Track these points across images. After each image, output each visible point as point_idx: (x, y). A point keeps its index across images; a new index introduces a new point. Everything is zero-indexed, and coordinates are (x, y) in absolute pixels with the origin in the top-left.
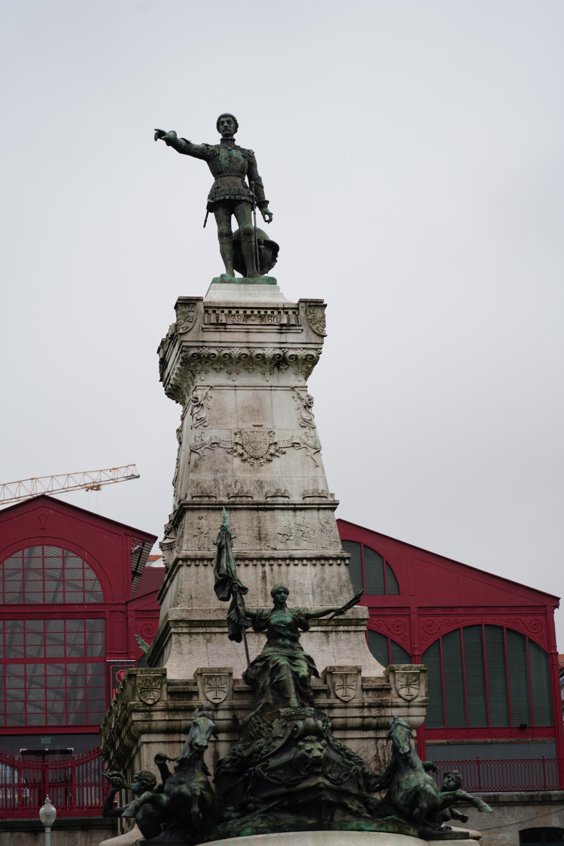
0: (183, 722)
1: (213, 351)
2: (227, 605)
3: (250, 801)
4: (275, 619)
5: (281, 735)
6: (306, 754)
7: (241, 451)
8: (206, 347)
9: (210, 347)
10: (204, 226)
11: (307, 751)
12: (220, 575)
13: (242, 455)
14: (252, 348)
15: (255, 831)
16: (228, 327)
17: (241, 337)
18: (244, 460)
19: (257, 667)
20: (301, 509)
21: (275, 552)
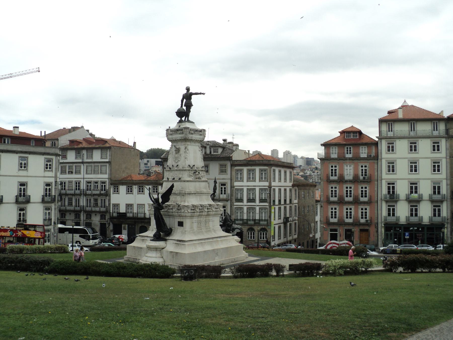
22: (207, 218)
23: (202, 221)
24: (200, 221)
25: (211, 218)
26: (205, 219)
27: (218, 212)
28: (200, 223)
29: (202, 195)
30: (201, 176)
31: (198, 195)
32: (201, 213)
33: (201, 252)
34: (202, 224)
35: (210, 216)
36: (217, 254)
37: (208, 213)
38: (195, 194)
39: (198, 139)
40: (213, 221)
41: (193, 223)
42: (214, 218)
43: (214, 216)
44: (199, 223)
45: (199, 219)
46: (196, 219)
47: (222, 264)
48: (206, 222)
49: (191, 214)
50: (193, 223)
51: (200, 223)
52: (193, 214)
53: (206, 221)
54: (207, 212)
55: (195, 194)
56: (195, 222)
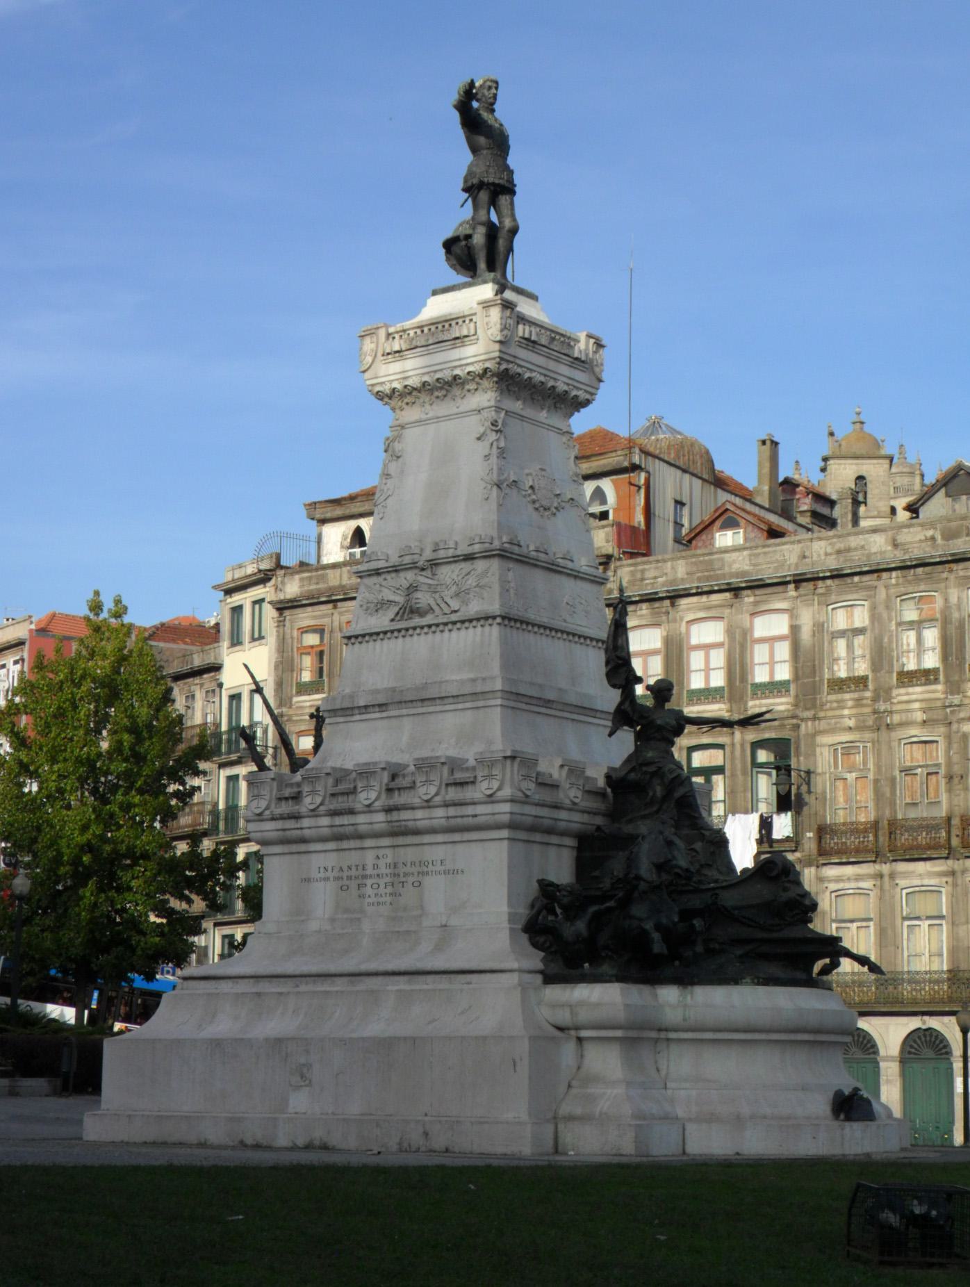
0: (545, 820)
1: (519, 370)
5: (711, 863)
6: (798, 898)
7: (534, 497)
8: (516, 364)
10: (462, 206)
11: (799, 895)
12: (619, 658)
13: (534, 502)
14: (548, 376)
15: (756, 981)
16: (537, 346)
17: (540, 360)
18: (537, 509)
19: (646, 773)
20: (582, 578)
21: (564, 624)
22: (409, 854)
23: (369, 871)
24: (353, 872)
25: (436, 852)
26: (389, 860)
27: (470, 810)
28: (353, 884)
29: (431, 709)
30: (457, 595)
31: (404, 712)
32: (345, 820)
34: (369, 891)
35: (427, 839)
36: (303, 1074)
37: (395, 816)
38: (382, 706)
40: (456, 872)
41: (307, 880)
42: (460, 848)
43: (457, 837)
45: (353, 858)
46: (331, 860)
47: (317, 1143)
48: (397, 878)
49: (279, 824)
50: (307, 880)
51: (353, 884)
52: (290, 824)
53: (402, 870)
54: (389, 810)
55: (382, 706)
56: (322, 875)
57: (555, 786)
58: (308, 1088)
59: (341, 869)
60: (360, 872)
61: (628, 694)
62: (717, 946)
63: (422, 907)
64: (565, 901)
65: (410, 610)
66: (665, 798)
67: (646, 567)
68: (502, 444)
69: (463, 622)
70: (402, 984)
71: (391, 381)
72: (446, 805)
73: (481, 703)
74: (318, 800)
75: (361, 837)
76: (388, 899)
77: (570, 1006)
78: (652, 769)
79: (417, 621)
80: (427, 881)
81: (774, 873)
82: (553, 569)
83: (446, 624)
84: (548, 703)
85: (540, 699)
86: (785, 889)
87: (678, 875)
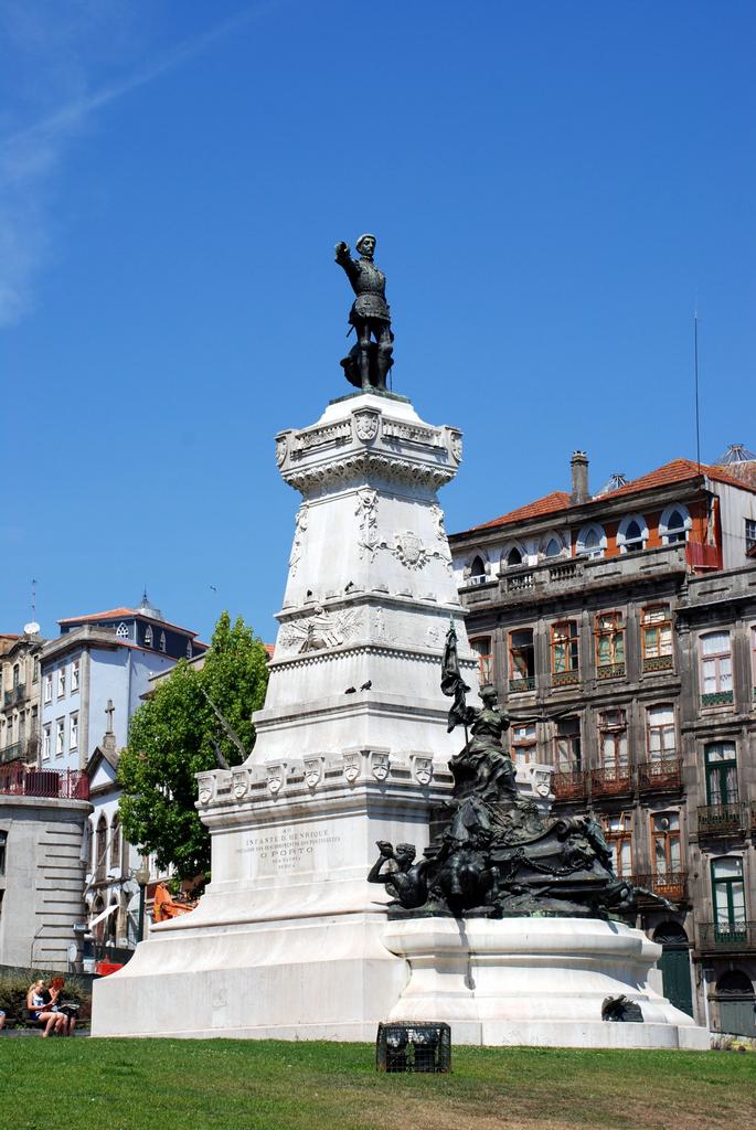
2: (452, 700)
3: (516, 884)
4: (486, 716)
7: (401, 554)
9: (385, 457)
13: (401, 558)
18: (404, 564)
22: (305, 828)
24: (269, 844)
26: (292, 833)
28: (269, 852)
29: (324, 718)
31: (307, 721)
32: (262, 804)
33: (151, 978)
34: (279, 857)
39: (333, 465)
40: (334, 839)
41: (240, 851)
44: (269, 851)
48: (298, 848)
51: (269, 852)
53: (301, 839)
56: (249, 847)
57: (406, 774)
58: (224, 1008)
59: (262, 842)
60: (274, 843)
61: (459, 701)
62: (519, 888)
63: (313, 868)
64: (400, 857)
65: (311, 644)
66: (490, 778)
67: (715, 581)
68: (373, 515)
69: (344, 652)
70: (291, 925)
71: (298, 473)
72: (326, 790)
73: (354, 712)
74: (243, 790)
75: (274, 819)
76: (292, 862)
77: (401, 936)
78: (480, 756)
79: (314, 653)
80: (317, 847)
81: (564, 831)
82: (416, 608)
83: (333, 654)
84: (410, 710)
85: (402, 707)
86: (571, 844)
87: (483, 836)
